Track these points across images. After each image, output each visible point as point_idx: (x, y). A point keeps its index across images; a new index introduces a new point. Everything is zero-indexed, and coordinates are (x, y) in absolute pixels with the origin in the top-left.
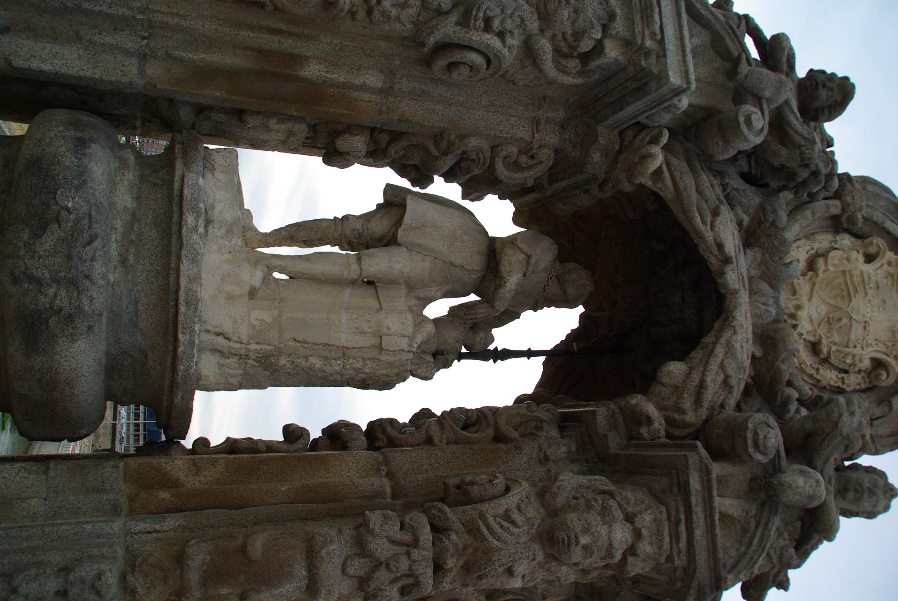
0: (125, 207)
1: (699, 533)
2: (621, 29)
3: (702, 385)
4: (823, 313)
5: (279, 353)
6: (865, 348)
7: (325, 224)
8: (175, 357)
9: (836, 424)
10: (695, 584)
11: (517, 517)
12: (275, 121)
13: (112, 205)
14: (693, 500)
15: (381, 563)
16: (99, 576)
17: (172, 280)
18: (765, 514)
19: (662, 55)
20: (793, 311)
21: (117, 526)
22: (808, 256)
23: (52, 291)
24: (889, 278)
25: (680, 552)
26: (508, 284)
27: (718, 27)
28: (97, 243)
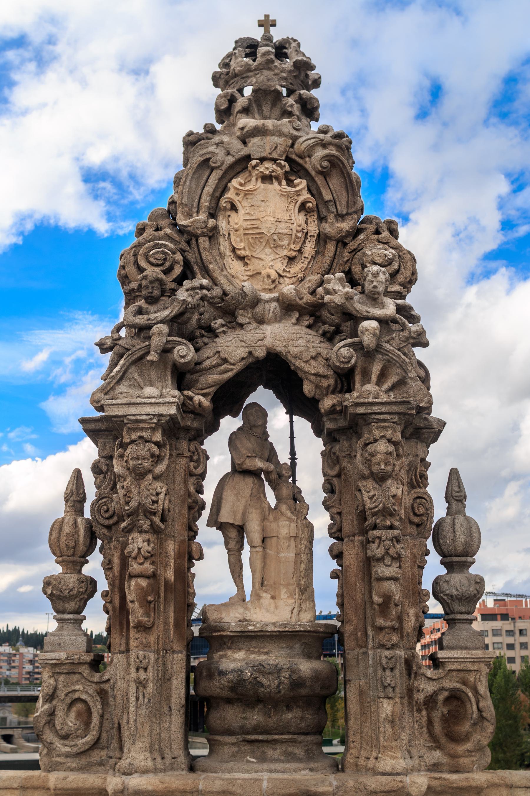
0: (245, 654)
1: (384, 409)
2: (148, 434)
3: (316, 375)
4: (270, 250)
5: (299, 585)
6: (292, 222)
7: (232, 559)
8: (305, 631)
9: (338, 305)
10: (406, 412)
11: (371, 494)
12: (190, 589)
13: (244, 659)
14: (369, 411)
15: (387, 552)
16: (386, 657)
17: (275, 634)
18: (382, 351)
19: (161, 415)
20: (270, 281)
21: (370, 652)
22: (235, 260)
23: (283, 679)
24: (248, 197)
25: (392, 419)
26: (261, 466)
27: (128, 364)
28: (263, 663)
